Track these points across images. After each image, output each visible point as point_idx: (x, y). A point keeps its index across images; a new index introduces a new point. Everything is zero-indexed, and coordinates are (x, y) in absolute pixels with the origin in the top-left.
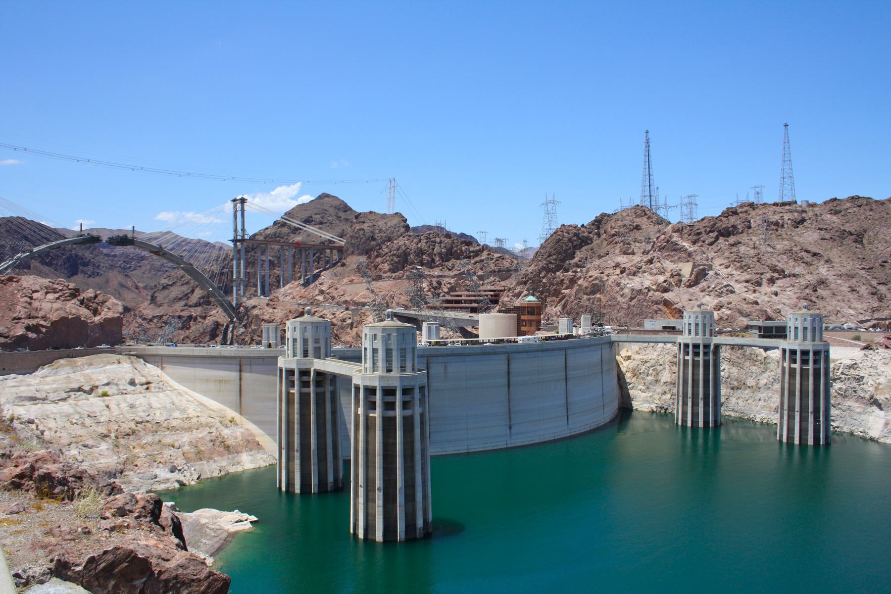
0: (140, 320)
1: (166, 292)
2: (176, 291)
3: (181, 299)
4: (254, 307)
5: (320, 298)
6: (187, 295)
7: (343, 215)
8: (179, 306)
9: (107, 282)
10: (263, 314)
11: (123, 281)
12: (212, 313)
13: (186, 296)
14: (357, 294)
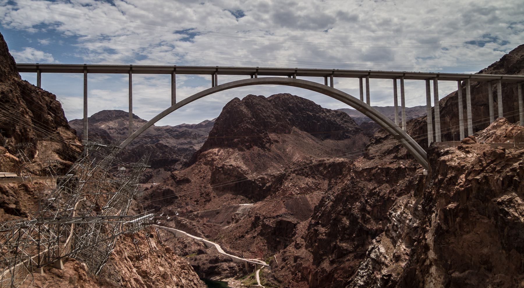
8: (388, 159)
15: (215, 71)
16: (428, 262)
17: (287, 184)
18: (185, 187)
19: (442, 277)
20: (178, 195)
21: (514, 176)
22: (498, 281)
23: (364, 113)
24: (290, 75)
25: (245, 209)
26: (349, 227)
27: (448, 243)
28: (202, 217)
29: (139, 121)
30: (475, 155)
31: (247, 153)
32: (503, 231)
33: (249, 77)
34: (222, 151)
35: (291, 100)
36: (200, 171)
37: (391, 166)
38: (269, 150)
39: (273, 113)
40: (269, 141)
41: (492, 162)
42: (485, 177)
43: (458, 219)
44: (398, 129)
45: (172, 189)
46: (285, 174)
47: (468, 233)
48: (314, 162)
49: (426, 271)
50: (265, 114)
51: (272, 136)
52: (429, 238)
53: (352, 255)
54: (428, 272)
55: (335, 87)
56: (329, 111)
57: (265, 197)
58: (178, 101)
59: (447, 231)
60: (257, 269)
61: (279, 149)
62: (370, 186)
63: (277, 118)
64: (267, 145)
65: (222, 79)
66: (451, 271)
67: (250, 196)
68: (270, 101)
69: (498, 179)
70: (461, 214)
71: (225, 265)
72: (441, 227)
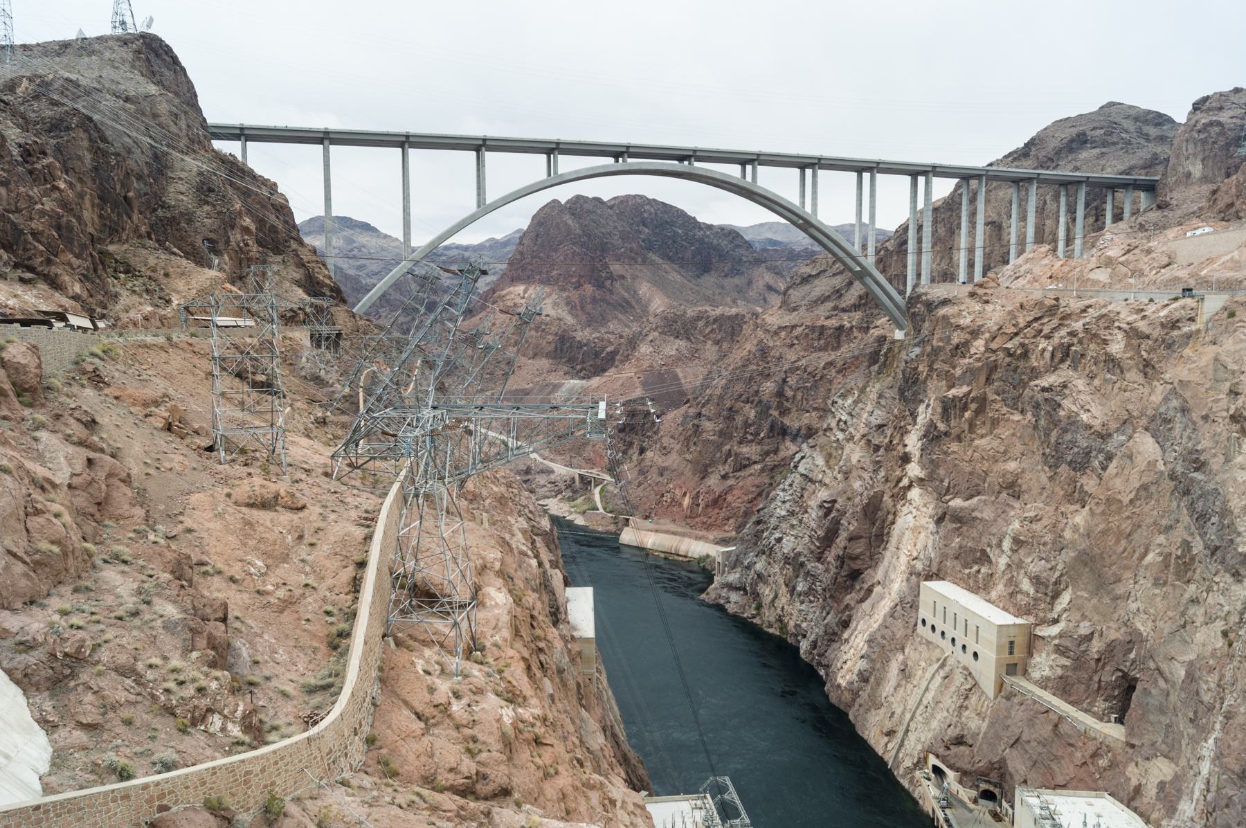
0: (760, 333)
1: (807, 287)
2: (822, 286)
3: (827, 298)
4: (945, 302)
5: (1102, 276)
6: (838, 291)
7: (1153, 131)
8: (823, 310)
9: (750, 283)
10: (959, 314)
11: (771, 282)
12: (879, 323)
13: (838, 293)
14: (1210, 261)
15: (552, 149)
16: (905, 482)
17: (644, 349)
19: (931, 506)
21: (1073, 345)
22: (1032, 514)
23: (805, 231)
24: (683, 161)
25: (572, 389)
26: (754, 423)
27: (945, 453)
29: (378, 236)
30: (998, 308)
31: (574, 295)
32: (1047, 435)
33: (611, 160)
34: (531, 291)
35: (647, 207)
36: (494, 324)
37: (828, 323)
38: (611, 291)
39: (615, 228)
40: (611, 277)
41: (1036, 319)
42: (1022, 345)
43: (967, 414)
44: (862, 260)
46: (640, 333)
47: (982, 437)
48: (690, 313)
49: (900, 495)
50: (603, 230)
51: (616, 268)
52: (913, 442)
53: (758, 467)
54: (904, 497)
55: (759, 183)
56: (710, 227)
57: (604, 370)
58: (490, 198)
59: (946, 434)
60: (596, 486)
61: (627, 290)
62: (791, 356)
63: (624, 237)
64: (608, 283)
65: (567, 164)
66: (947, 498)
67: (579, 367)
68: (611, 207)
69: (1044, 350)
70: (973, 406)
71: (541, 479)
72: (936, 427)
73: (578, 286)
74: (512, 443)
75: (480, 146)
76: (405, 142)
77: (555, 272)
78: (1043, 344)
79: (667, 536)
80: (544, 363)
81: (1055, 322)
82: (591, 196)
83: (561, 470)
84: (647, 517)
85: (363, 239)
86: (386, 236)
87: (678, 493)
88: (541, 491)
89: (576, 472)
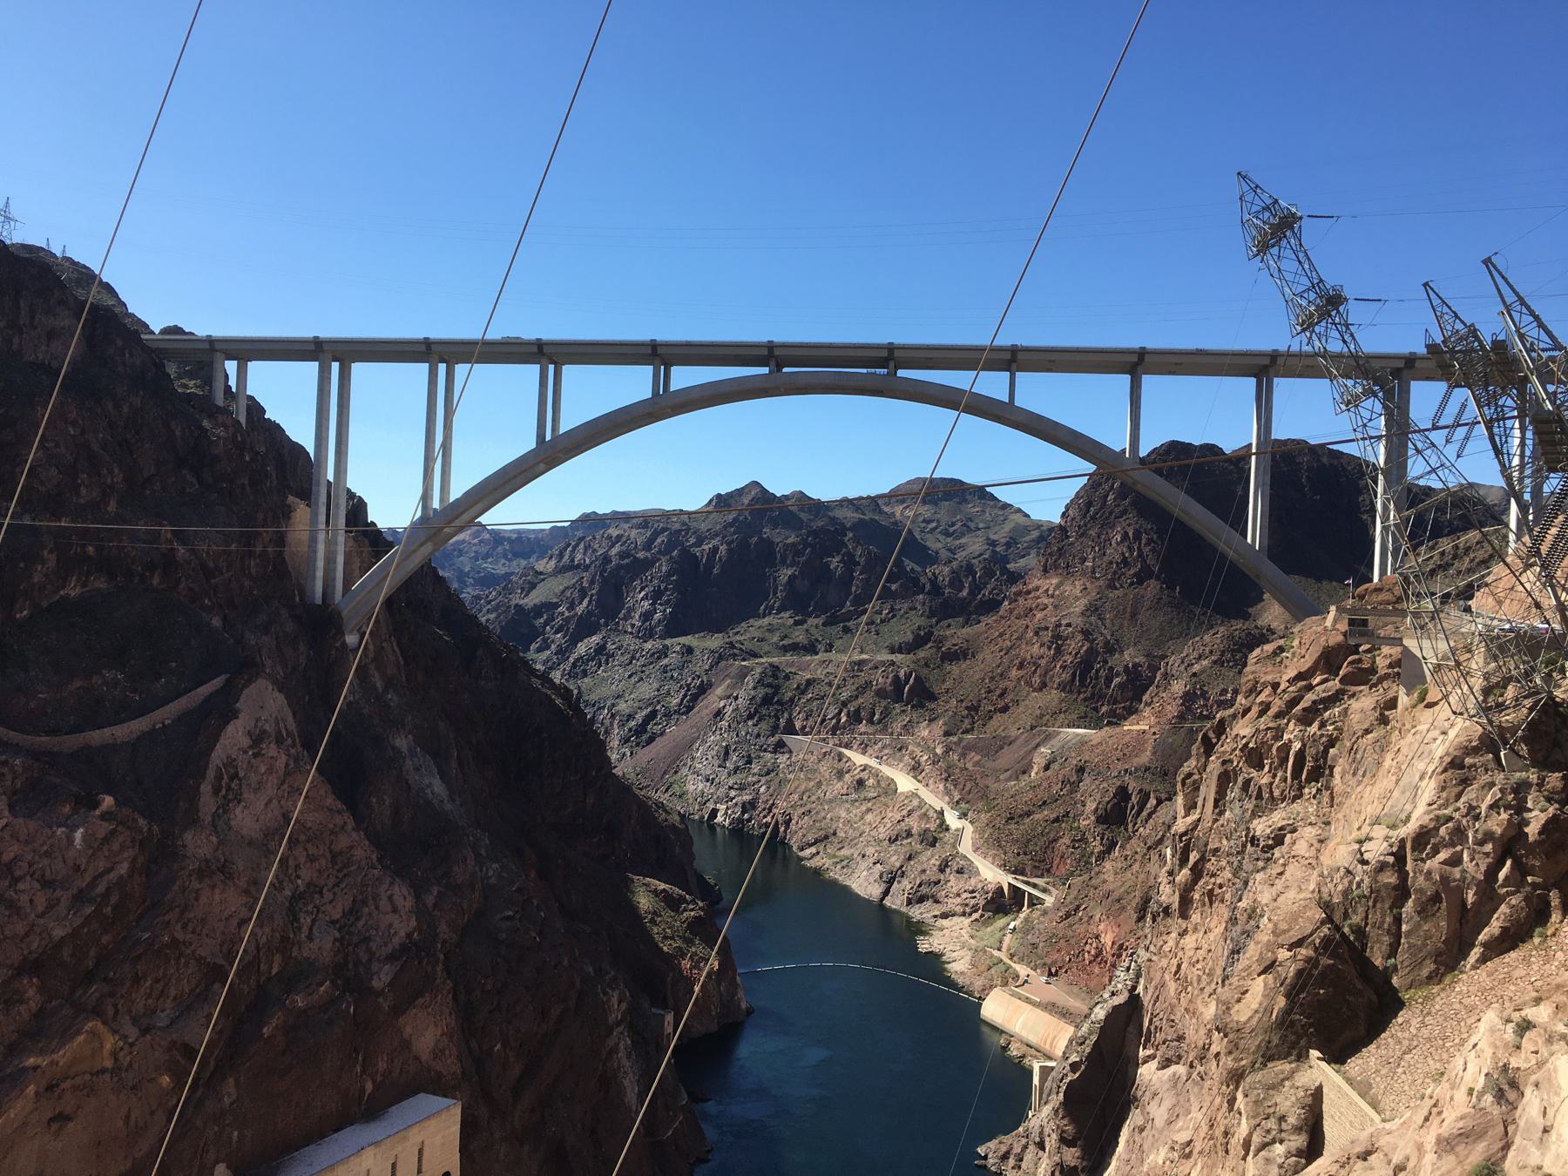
18: (955, 669)
20: (936, 690)
28: (969, 748)
34: (1067, 587)
41: (1300, 676)
45: (925, 672)
47: (1195, 930)
65: (684, 377)
67: (1104, 709)
71: (954, 883)
73: (1140, 579)
74: (952, 819)
75: (549, 355)
76: (437, 354)
77: (1106, 559)
78: (1292, 732)
79: (1045, 1016)
80: (1053, 696)
81: (1335, 684)
82: (1197, 442)
83: (992, 874)
84: (1050, 974)
85: (973, 508)
86: (1006, 506)
87: (1107, 939)
88: (953, 904)
89: (1005, 880)
